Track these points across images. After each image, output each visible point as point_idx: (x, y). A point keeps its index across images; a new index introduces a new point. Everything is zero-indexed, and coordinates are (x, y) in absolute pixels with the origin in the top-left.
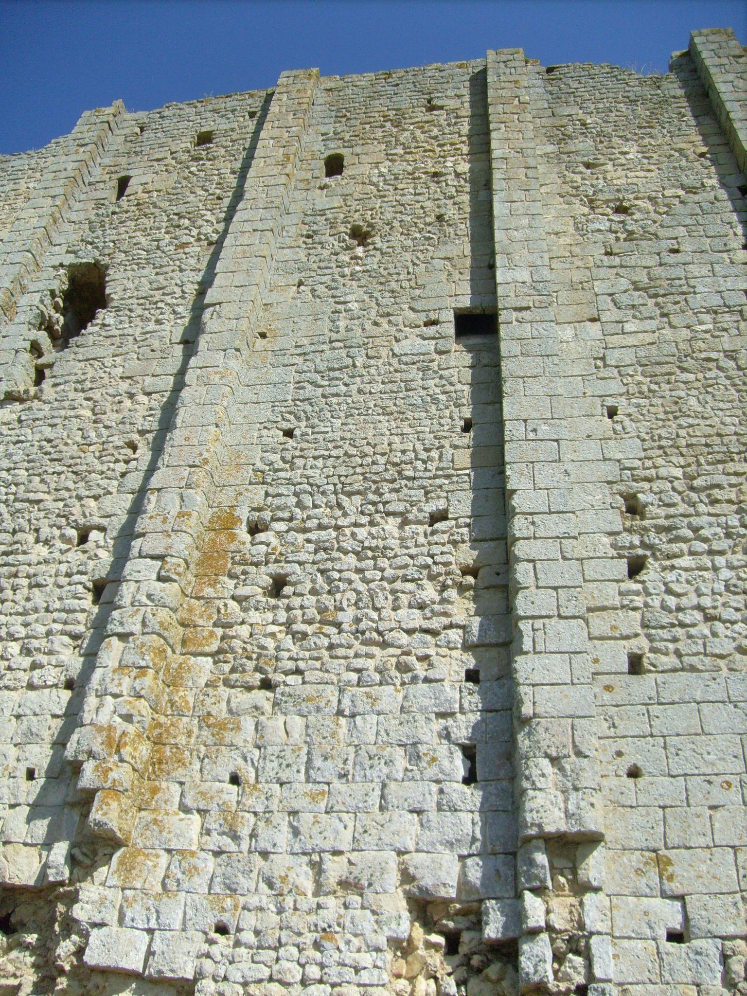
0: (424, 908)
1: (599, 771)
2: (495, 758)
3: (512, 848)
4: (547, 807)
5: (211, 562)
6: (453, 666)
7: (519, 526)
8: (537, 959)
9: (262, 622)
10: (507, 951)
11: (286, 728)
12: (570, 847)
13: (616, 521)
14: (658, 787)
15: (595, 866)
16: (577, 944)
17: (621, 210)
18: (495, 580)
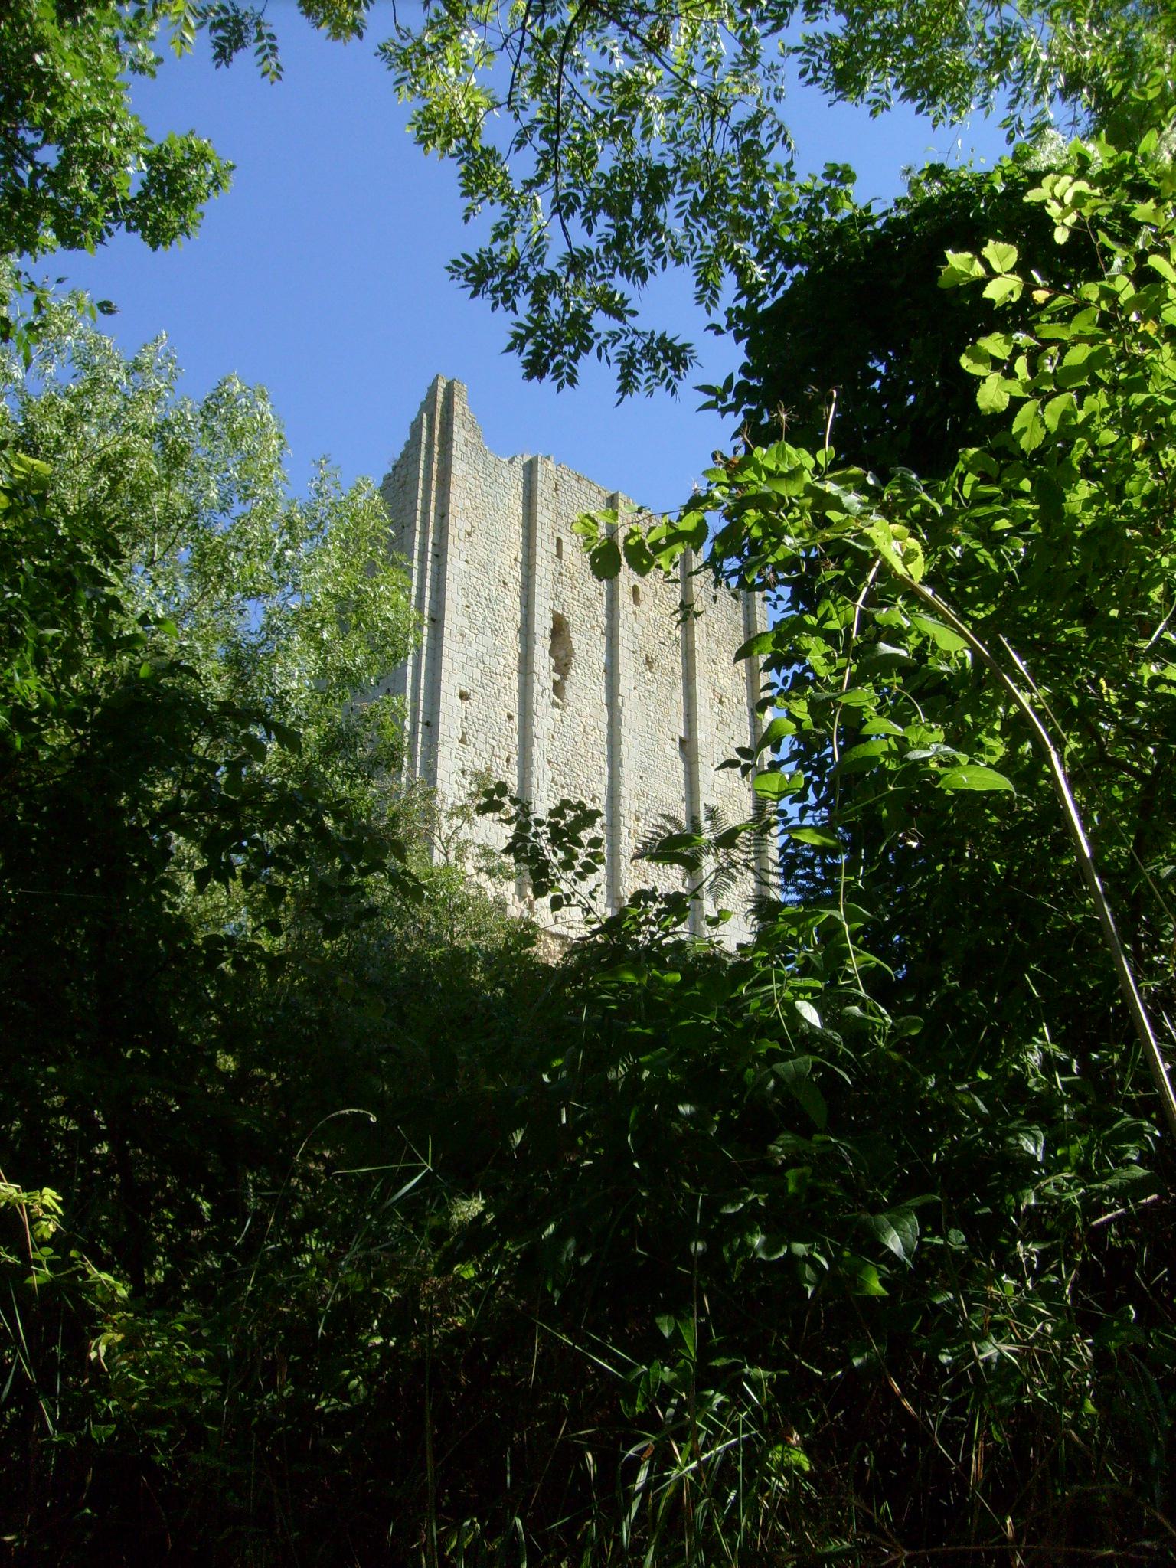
17: (721, 702)
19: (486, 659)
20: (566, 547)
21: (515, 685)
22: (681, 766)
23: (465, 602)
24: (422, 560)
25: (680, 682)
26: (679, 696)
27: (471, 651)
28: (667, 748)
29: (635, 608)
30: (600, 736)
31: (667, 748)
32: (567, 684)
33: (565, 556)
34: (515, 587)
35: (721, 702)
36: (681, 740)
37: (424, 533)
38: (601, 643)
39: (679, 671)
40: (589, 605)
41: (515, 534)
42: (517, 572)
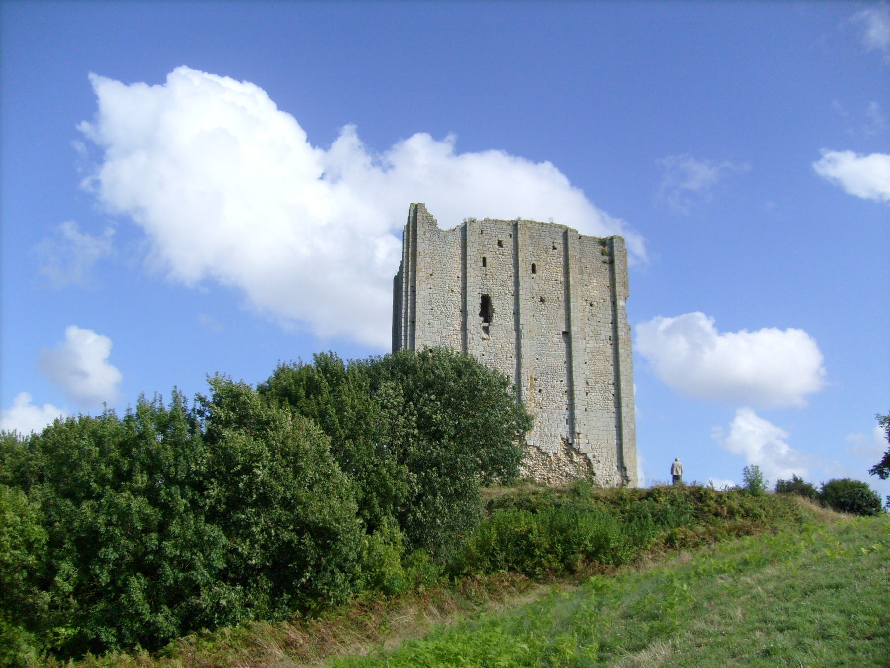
0: (562, 439)
1: (583, 426)
2: (571, 420)
3: (572, 432)
4: (577, 430)
5: (532, 386)
6: (565, 407)
7: (575, 388)
8: (574, 446)
9: (539, 397)
10: (571, 444)
11: (545, 415)
12: (578, 434)
13: (585, 385)
14: (587, 427)
15: (581, 436)
16: (579, 444)
18: (570, 393)
19: (443, 330)
20: (487, 261)
21: (460, 337)
22: (564, 345)
23: (430, 307)
24: (407, 296)
25: (563, 304)
26: (562, 311)
27: (435, 330)
28: (555, 340)
29: (533, 275)
30: (511, 347)
31: (555, 340)
32: (490, 327)
33: (487, 265)
34: (458, 290)
35: (591, 305)
36: (563, 332)
37: (407, 283)
38: (510, 300)
39: (562, 298)
40: (503, 283)
41: (457, 264)
42: (460, 283)
